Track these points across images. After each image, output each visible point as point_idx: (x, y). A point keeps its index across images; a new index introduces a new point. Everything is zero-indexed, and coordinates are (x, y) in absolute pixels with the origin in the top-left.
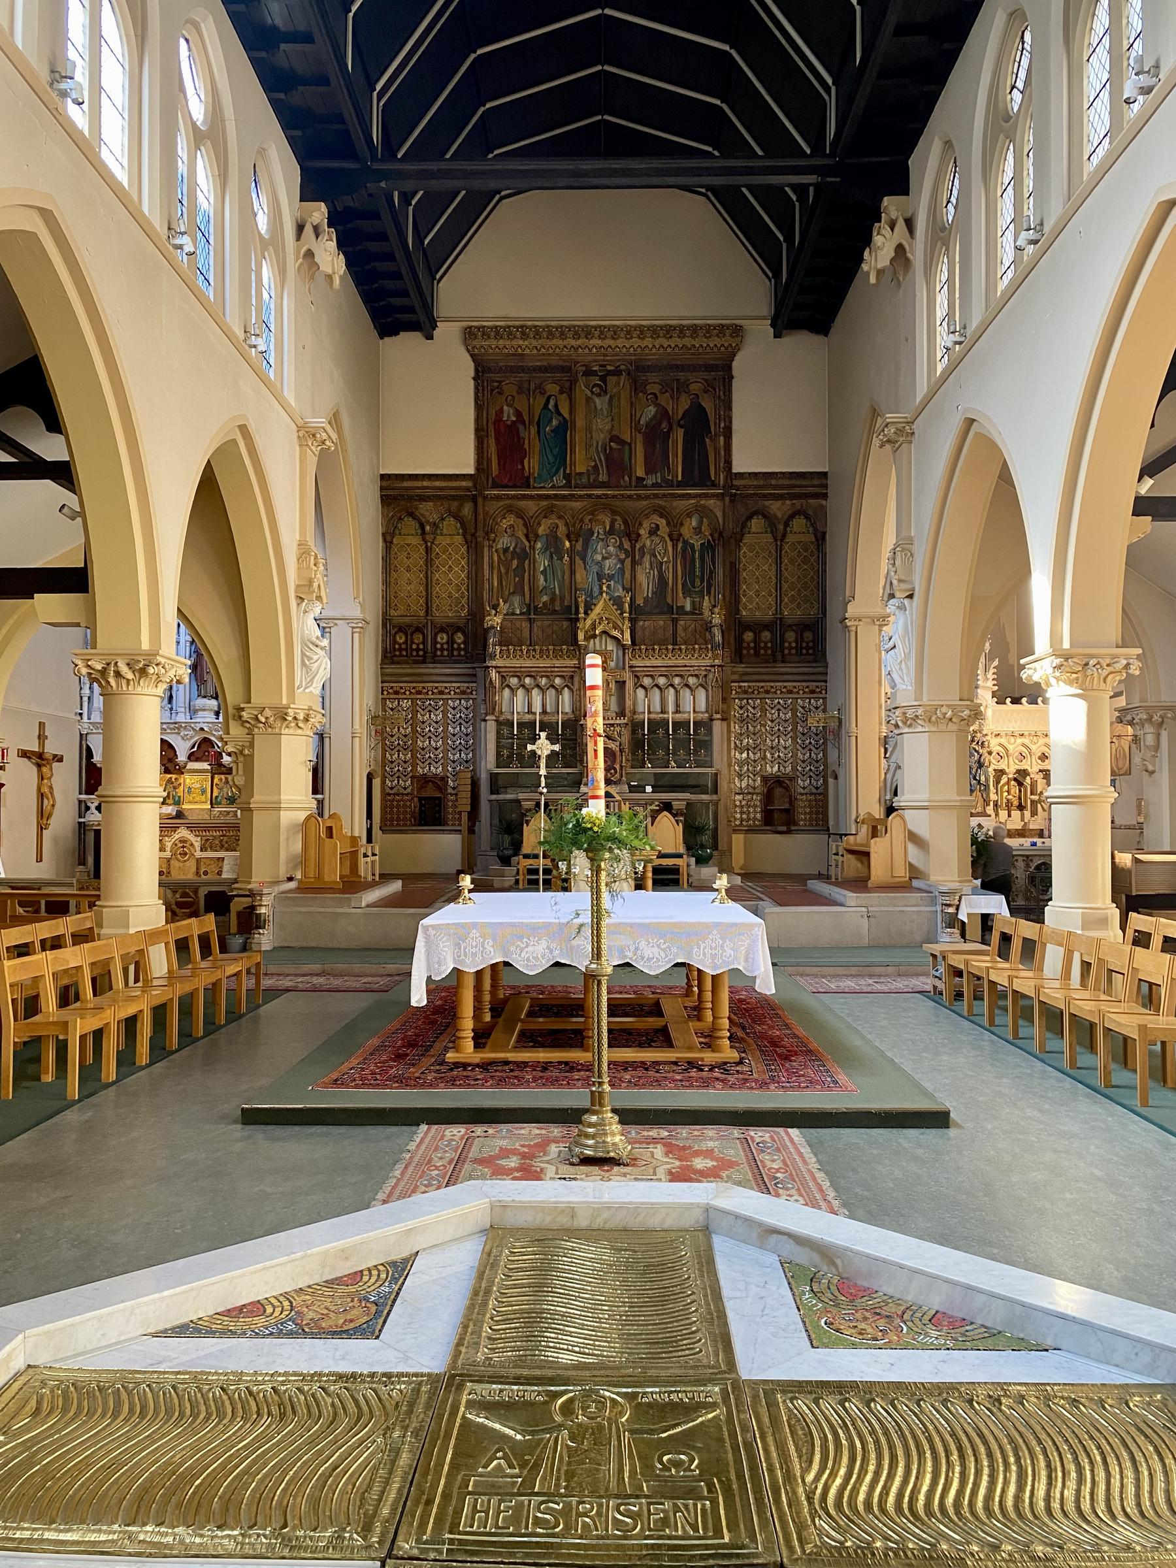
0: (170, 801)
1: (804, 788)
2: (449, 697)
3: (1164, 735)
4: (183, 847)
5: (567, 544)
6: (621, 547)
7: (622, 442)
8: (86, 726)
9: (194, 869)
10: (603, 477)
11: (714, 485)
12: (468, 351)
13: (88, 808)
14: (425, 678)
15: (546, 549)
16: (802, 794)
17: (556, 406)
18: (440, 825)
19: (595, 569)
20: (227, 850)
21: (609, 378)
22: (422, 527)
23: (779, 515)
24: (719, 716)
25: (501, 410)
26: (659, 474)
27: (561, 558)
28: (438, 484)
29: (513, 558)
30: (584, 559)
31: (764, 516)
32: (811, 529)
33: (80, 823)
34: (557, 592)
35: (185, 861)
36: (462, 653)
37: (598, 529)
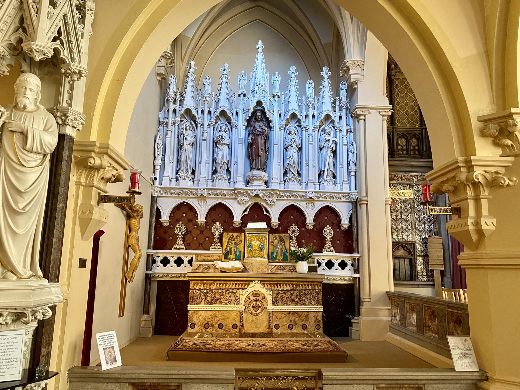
0: (232, 256)
4: (256, 300)
8: (157, 190)
9: (266, 323)
14: (396, 169)
20: (297, 304)
33: (147, 275)
35: (257, 315)
36: (417, 153)
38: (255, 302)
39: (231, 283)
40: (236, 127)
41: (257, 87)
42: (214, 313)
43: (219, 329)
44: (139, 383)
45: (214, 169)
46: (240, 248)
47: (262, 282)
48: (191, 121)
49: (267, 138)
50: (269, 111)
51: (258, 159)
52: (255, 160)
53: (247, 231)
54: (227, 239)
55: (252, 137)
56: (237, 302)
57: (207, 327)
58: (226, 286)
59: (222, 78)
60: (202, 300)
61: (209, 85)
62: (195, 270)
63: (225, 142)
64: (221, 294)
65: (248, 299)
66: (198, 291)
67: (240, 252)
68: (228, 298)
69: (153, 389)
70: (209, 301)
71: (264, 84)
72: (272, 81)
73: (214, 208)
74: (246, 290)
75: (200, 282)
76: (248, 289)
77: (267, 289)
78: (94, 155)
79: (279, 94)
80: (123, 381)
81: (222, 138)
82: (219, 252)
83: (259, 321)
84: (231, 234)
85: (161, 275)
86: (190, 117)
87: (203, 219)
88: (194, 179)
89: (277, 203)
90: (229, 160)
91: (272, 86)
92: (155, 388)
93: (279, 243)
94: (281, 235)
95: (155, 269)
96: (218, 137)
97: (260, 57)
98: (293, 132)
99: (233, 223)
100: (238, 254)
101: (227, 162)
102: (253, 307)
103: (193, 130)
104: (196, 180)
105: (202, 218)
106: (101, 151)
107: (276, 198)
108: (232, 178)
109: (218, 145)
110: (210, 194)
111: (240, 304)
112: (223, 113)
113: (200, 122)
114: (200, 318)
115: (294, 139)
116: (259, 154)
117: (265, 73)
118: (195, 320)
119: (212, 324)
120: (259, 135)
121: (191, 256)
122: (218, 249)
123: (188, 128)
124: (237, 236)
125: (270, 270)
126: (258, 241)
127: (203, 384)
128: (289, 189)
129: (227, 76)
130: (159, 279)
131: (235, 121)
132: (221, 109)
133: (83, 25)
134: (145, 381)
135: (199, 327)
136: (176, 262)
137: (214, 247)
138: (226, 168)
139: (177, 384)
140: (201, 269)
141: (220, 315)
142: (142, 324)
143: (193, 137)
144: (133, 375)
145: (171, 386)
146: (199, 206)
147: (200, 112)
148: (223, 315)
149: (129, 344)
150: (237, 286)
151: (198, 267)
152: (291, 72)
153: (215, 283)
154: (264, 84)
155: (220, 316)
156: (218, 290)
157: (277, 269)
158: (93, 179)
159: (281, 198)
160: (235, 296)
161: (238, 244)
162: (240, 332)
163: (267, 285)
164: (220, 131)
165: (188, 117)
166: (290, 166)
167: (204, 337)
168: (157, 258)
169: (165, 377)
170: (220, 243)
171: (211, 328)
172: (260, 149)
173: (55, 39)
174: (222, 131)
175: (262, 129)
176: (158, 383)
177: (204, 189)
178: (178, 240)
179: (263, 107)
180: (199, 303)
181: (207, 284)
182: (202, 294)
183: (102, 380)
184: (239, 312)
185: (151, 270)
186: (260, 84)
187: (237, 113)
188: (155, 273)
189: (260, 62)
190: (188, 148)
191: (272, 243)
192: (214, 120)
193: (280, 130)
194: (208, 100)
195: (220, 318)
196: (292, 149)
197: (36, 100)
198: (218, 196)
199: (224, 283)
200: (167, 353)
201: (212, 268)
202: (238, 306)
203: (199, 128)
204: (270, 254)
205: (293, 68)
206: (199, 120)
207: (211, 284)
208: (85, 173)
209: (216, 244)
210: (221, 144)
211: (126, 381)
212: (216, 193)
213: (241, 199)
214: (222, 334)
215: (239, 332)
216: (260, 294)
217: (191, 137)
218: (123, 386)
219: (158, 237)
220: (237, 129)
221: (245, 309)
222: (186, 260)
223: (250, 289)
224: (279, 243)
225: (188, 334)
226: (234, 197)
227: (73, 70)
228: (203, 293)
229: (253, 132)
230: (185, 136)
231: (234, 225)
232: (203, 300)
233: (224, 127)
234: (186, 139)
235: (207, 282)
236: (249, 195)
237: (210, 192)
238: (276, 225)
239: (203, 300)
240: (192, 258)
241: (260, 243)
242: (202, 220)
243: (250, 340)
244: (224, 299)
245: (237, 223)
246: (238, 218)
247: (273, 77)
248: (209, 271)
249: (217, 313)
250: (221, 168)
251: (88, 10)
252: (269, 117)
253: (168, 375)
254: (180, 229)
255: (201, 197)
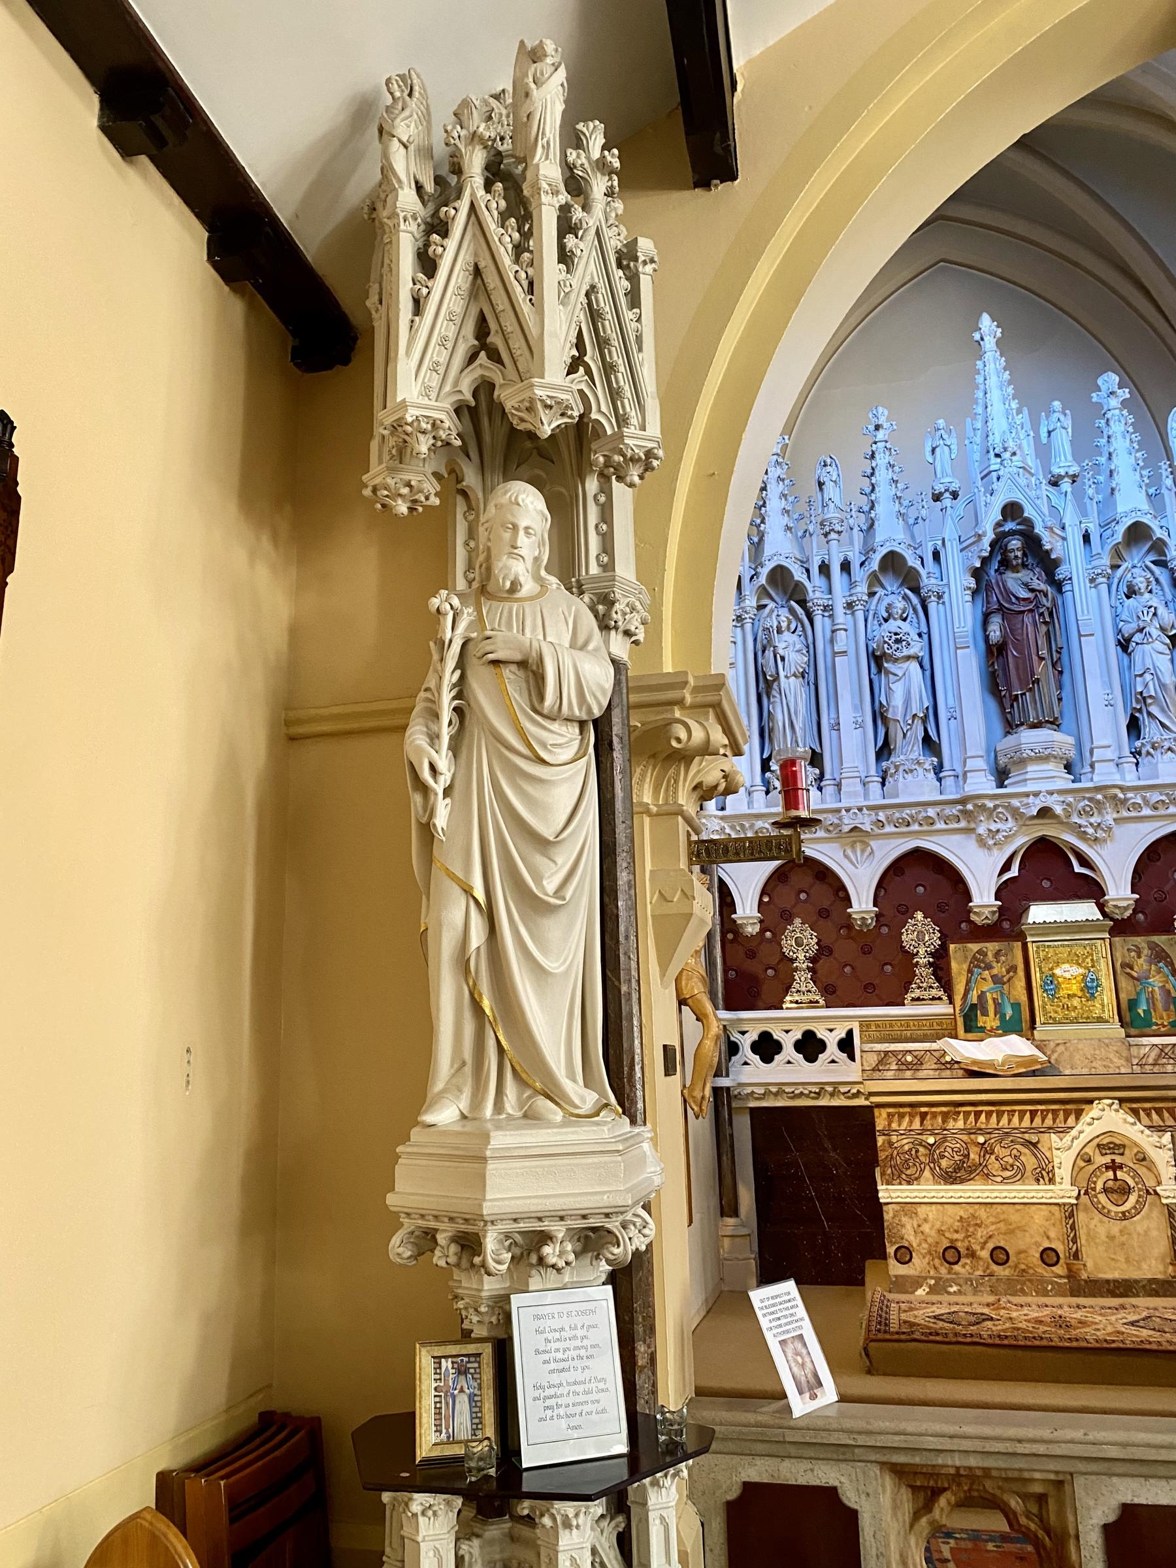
4: (1114, 1167)
35: (1125, 1216)
38: (1110, 1174)
39: (1015, 1111)
40: (940, 597)
41: (999, 460)
42: (971, 1211)
43: (994, 1267)
44: (918, 1465)
45: (880, 743)
46: (1014, 993)
47: (1128, 1105)
48: (792, 603)
49: (1051, 618)
50: (1051, 529)
51: (1030, 690)
52: (1022, 695)
53: (1032, 935)
54: (965, 967)
55: (1001, 621)
56: (1043, 1172)
57: (951, 1260)
58: (998, 1122)
59: (873, 453)
60: (922, 1171)
61: (835, 482)
62: (873, 1070)
63: (911, 651)
64: (986, 1150)
65: (1083, 1164)
66: (905, 1141)
67: (1016, 1006)
68: (1011, 1161)
69: (966, 1488)
70: (947, 1173)
71: (1020, 448)
72: (1044, 435)
73: (897, 868)
74: (1074, 1132)
75: (908, 1110)
76: (1079, 1128)
77: (1149, 1127)
78: (681, 715)
79: (1074, 469)
80: (864, 1458)
81: (898, 641)
82: (942, 1008)
83: (1135, 1236)
84: (974, 947)
85: (760, 1090)
86: (785, 593)
87: (867, 903)
88: (821, 781)
89: (1118, 831)
90: (927, 708)
91: (1044, 452)
92: (975, 1487)
93: (1153, 967)
94: (1155, 939)
95: (739, 1073)
96: (887, 639)
97: (992, 366)
98: (1143, 586)
99: (970, 911)
100: (1009, 1012)
101: (922, 715)
102: (1106, 1190)
103: (800, 628)
104: (828, 782)
105: (862, 904)
106: (701, 698)
107: (1115, 815)
108: (947, 765)
109: (886, 665)
110: (880, 824)
111: (1058, 1179)
112: (892, 562)
113: (820, 602)
114: (926, 1228)
115: (1153, 609)
116: (1033, 674)
117: (1014, 411)
118: (910, 1236)
119: (968, 1249)
120: (1023, 612)
121: (847, 1026)
122: (933, 999)
123: (784, 625)
124: (997, 954)
125: (1135, 1061)
126: (1075, 967)
127: (1152, 1481)
128: (1157, 777)
129: (888, 446)
130: (752, 1104)
131: (933, 581)
132: (884, 551)
133: (638, 311)
134: (940, 1461)
135: (927, 1260)
136: (799, 1046)
137: (917, 993)
138: (921, 734)
139: (1052, 1477)
140: (894, 1067)
141: (992, 1219)
142: (723, 1247)
143: (804, 652)
144: (897, 1438)
145: (1032, 1480)
146: (846, 863)
147: (815, 571)
148: (1002, 1217)
149: (703, 1313)
150: (1038, 1120)
151: (880, 1062)
152: (1104, 393)
153: (959, 1113)
154: (1020, 448)
155: (993, 1224)
156: (973, 1136)
157: (1159, 1056)
158: (675, 792)
159: (1133, 814)
160: (1036, 1157)
161: (1005, 979)
162: (1071, 1275)
163: (1149, 1115)
164: (886, 620)
165: (777, 594)
166: (1149, 701)
167: (949, 1293)
168: (739, 1036)
169: (1010, 1450)
170: (938, 979)
171: (968, 1261)
172: (1035, 658)
173: (572, 370)
174: (895, 619)
175: (1032, 590)
176: (983, 1469)
177: (860, 809)
178: (796, 977)
179: (1029, 523)
180: (916, 1179)
181: (934, 1115)
182: (921, 1149)
183: (793, 1450)
184: (1057, 1208)
185: (727, 1075)
186: (1005, 449)
187: (936, 556)
188: (740, 1085)
189: (993, 381)
190: (792, 688)
191: (1128, 970)
192: (862, 589)
193: (1095, 587)
194: (838, 528)
195: (993, 1227)
196: (1148, 643)
197: (537, 560)
198: (908, 825)
199: (992, 1112)
200: (865, 1349)
201: (930, 1063)
202: (1051, 1187)
203: (818, 620)
204: (1124, 1005)
205: (1110, 380)
206: (818, 594)
207: (945, 1116)
208: (652, 775)
209: (925, 985)
210: (896, 660)
211: (873, 1458)
212: (903, 819)
213: (990, 830)
214: (1009, 1280)
215: (1068, 1277)
216: (1124, 1146)
217: (798, 651)
218: (864, 1473)
219: (733, 970)
220: (944, 603)
221: (1077, 1198)
222: (832, 1041)
223: (1088, 1129)
224: (1153, 967)
225: (892, 1282)
226: (963, 824)
227: (629, 454)
228: (924, 1146)
229: (1000, 604)
230: (781, 652)
231: (973, 917)
232: (927, 1167)
233: (900, 604)
234: (783, 659)
235: (934, 1109)
236: (1016, 813)
237: (882, 816)
238: (1126, 908)
239: (927, 1167)
240: (850, 1033)
241: (1082, 971)
242: (864, 907)
243: (1123, 1307)
244: (997, 1165)
245: (986, 911)
246: (986, 893)
247: (1044, 422)
248: (921, 1074)
249: (982, 1213)
250: (905, 735)
251: (645, 263)
252: (1051, 550)
253: (1020, 1441)
254: (799, 943)
255: (852, 834)
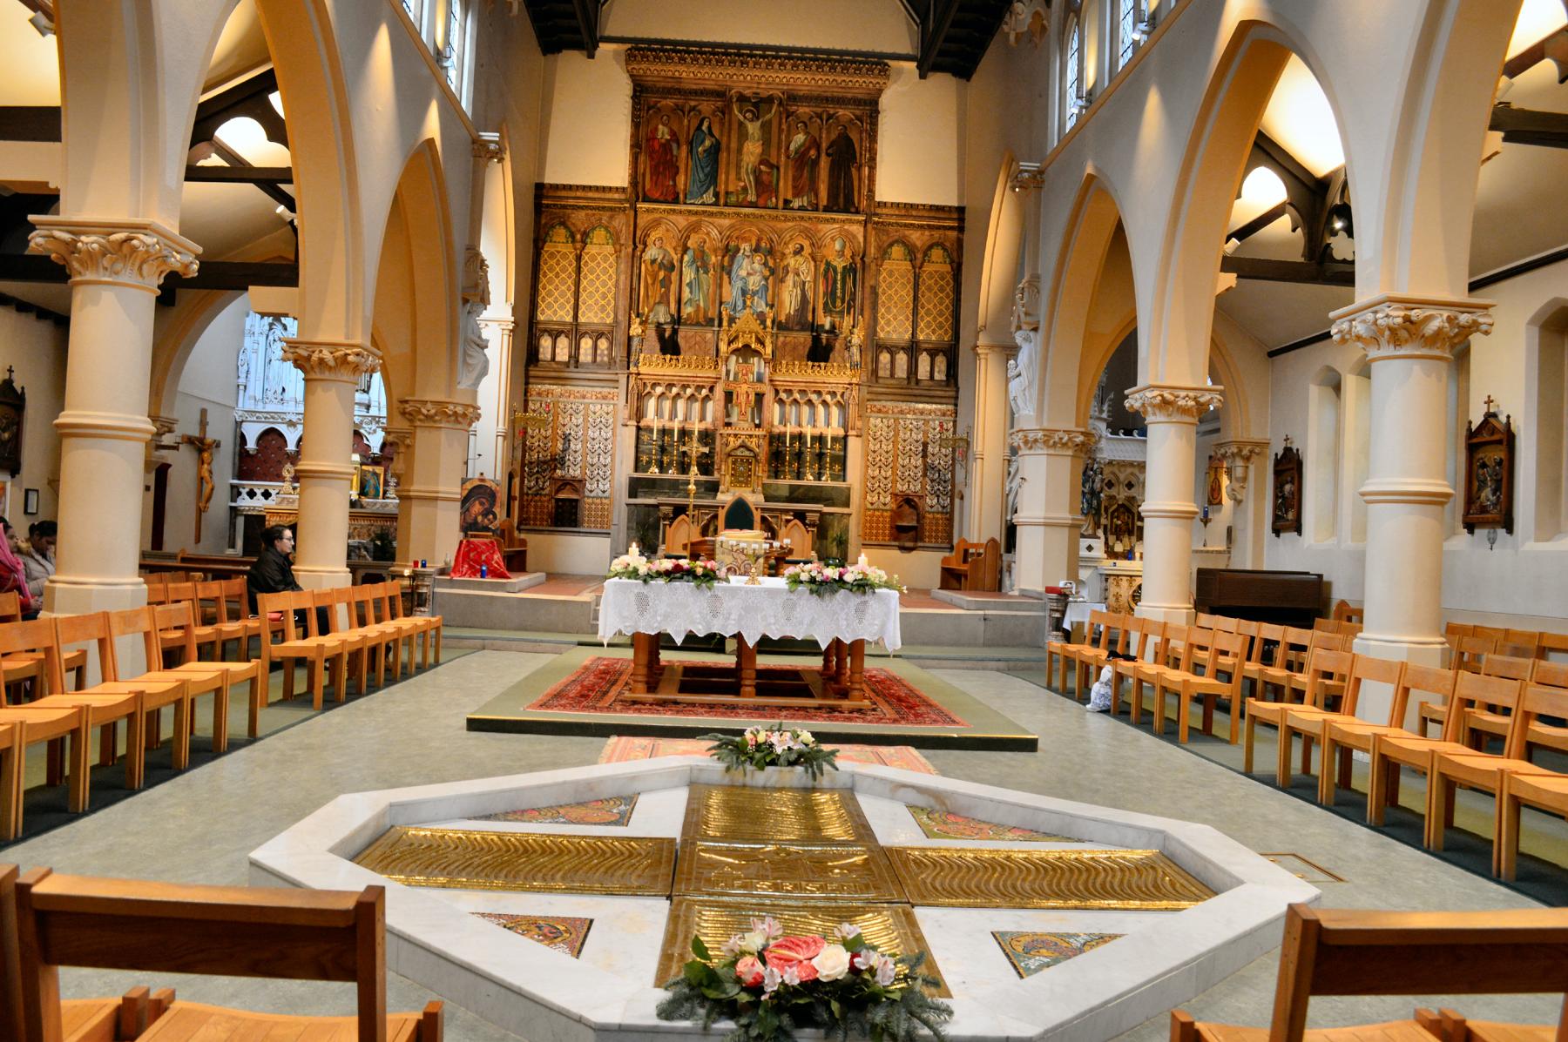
1: (932, 507)
2: (590, 401)
3: (1252, 467)
5: (713, 258)
6: (765, 264)
7: (771, 166)
10: (752, 197)
11: (857, 212)
12: (628, 71)
13: (240, 494)
15: (694, 261)
16: (929, 513)
17: (709, 128)
18: (575, 526)
19: (739, 284)
21: (762, 105)
22: (573, 236)
23: (919, 244)
24: (854, 433)
25: (656, 129)
26: (805, 198)
27: (706, 272)
28: (590, 195)
29: (660, 269)
30: (729, 274)
31: (903, 243)
32: (948, 260)
33: (231, 508)
34: (702, 304)
37: (745, 247)
136: (263, 494)
222: (273, 492)
